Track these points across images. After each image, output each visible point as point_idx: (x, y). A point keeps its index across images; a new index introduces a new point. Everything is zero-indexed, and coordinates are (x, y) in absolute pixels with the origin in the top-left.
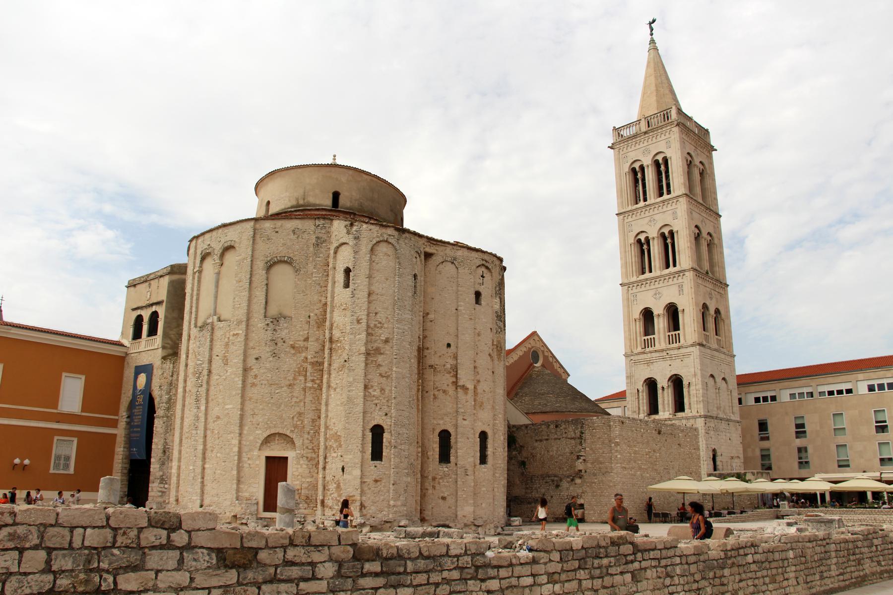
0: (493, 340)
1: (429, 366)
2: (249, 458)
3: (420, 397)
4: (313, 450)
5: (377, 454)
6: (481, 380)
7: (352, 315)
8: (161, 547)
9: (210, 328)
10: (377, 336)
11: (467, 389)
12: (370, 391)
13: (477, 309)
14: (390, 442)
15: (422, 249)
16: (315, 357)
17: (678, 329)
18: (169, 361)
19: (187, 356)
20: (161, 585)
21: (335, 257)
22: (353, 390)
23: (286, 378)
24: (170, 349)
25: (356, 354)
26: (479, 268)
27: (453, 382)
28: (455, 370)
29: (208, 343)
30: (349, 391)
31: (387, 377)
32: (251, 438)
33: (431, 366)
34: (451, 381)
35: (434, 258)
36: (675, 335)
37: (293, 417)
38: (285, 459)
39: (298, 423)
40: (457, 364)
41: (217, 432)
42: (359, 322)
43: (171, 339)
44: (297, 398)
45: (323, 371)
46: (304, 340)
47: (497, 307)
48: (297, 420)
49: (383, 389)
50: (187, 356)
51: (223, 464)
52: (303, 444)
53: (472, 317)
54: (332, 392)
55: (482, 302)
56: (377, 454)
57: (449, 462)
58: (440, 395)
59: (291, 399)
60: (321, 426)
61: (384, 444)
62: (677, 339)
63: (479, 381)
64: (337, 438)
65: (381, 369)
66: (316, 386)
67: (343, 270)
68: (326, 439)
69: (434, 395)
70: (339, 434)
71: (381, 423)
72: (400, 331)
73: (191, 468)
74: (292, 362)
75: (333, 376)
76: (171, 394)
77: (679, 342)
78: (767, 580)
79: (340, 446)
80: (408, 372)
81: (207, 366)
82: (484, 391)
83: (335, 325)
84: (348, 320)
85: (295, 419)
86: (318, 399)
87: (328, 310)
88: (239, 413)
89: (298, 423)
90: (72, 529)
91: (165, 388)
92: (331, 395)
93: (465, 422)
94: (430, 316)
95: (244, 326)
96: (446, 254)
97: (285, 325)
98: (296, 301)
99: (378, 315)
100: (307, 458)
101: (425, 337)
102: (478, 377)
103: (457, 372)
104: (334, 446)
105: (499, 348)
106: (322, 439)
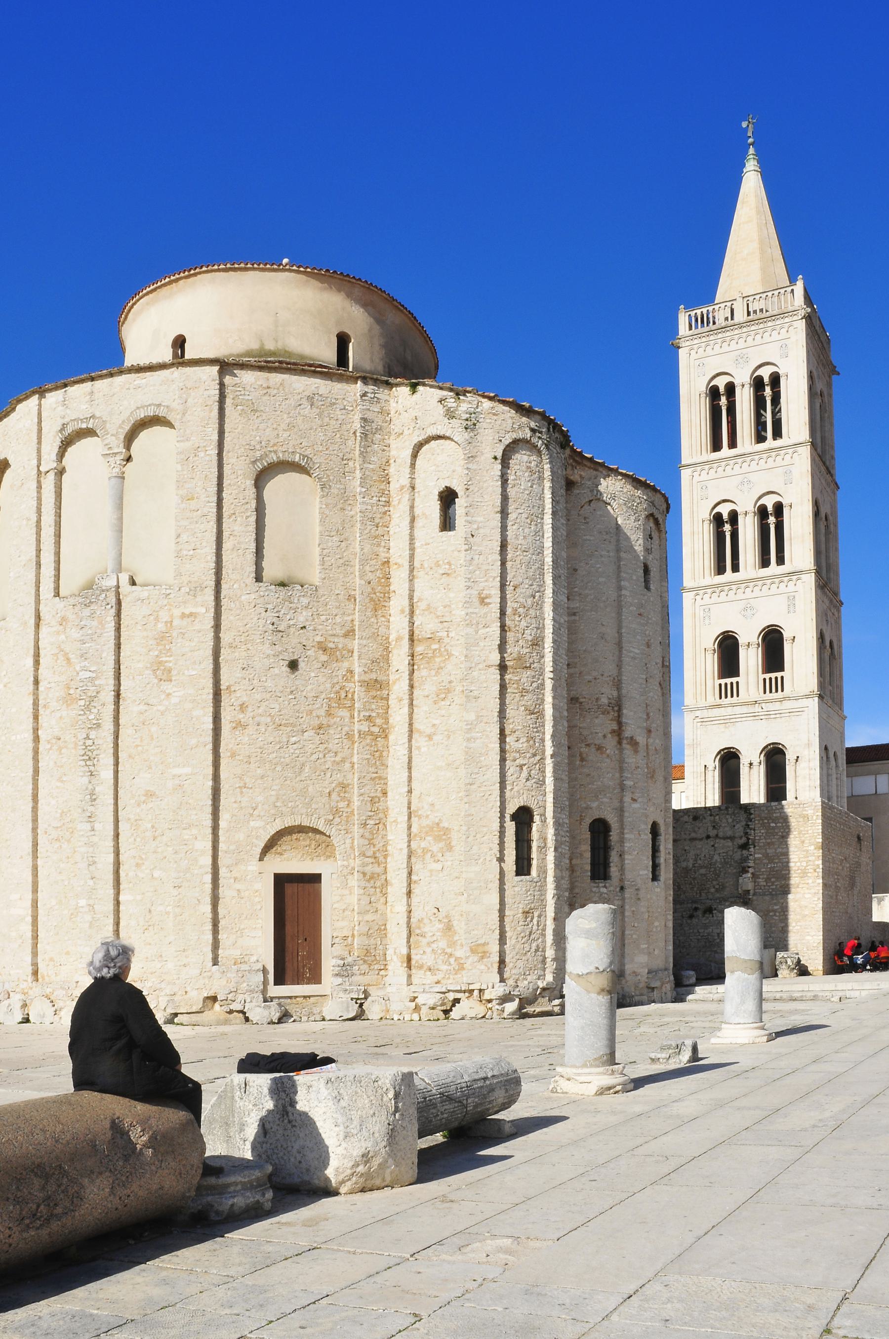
2: (235, 879)
6: (652, 729)
7: (468, 588)
11: (638, 743)
16: (371, 670)
17: (782, 669)
22: (475, 739)
23: (311, 712)
25: (481, 666)
27: (613, 732)
28: (617, 706)
30: (468, 740)
32: (241, 836)
34: (610, 729)
36: (776, 678)
37: (329, 793)
38: (316, 878)
39: (342, 805)
41: (150, 825)
42: (483, 601)
45: (387, 699)
46: (346, 635)
48: (339, 798)
51: (175, 892)
58: (592, 755)
59: (324, 756)
62: (778, 686)
64: (442, 833)
69: (581, 754)
73: (83, 902)
74: (321, 679)
77: (782, 690)
85: (334, 796)
86: (381, 756)
89: (342, 805)
92: (419, 748)
97: (305, 601)
98: (325, 552)
103: (620, 710)
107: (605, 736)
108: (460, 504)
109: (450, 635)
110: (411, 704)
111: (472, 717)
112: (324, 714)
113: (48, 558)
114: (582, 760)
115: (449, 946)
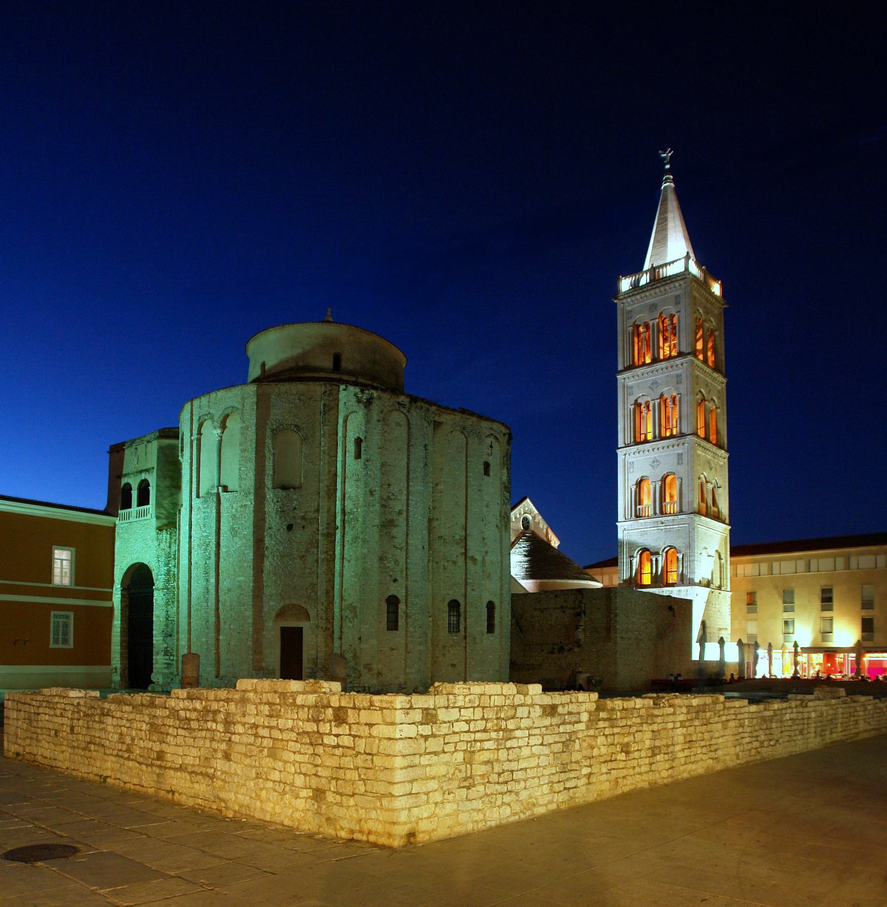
0: (501, 512)
1: (439, 537)
3: (430, 567)
4: (328, 620)
5: (393, 625)
8: (522, 705)
9: (215, 499)
10: (391, 508)
11: (476, 560)
12: (385, 562)
13: (486, 480)
14: (406, 613)
15: (431, 418)
18: (164, 531)
19: (190, 528)
20: (522, 726)
21: (345, 427)
24: (164, 519)
26: (488, 438)
27: (462, 553)
29: (214, 515)
31: (401, 549)
33: (440, 537)
35: (443, 427)
38: (300, 630)
40: (466, 534)
42: (371, 493)
43: (164, 508)
44: (310, 569)
46: (315, 512)
47: (505, 478)
49: (396, 562)
50: (190, 528)
52: (317, 615)
53: (481, 488)
54: (346, 563)
55: (491, 474)
56: (393, 625)
57: (459, 631)
60: (335, 597)
61: (399, 614)
63: (487, 552)
65: (395, 540)
66: (329, 557)
67: (353, 439)
68: (341, 610)
69: (444, 566)
70: (354, 604)
71: (395, 593)
72: (413, 503)
75: (346, 547)
76: (171, 565)
78: (797, 732)
79: (356, 616)
80: (421, 544)
81: (214, 537)
82: (491, 562)
83: (347, 496)
84: (361, 491)
85: (309, 591)
87: (339, 480)
88: (252, 584)
89: (313, 594)
90: (490, 696)
91: (162, 559)
93: (473, 593)
94: (439, 487)
95: (252, 497)
96: (455, 423)
99: (391, 487)
100: (322, 628)
101: (434, 508)
102: (486, 549)
103: (466, 543)
104: (350, 616)
105: (506, 520)
106: (337, 610)
107: (457, 556)
108: (363, 445)
109: (359, 510)
110: (344, 546)
111: (366, 551)
112: (304, 550)
113: (194, 480)
114: (445, 568)
115: (355, 665)
